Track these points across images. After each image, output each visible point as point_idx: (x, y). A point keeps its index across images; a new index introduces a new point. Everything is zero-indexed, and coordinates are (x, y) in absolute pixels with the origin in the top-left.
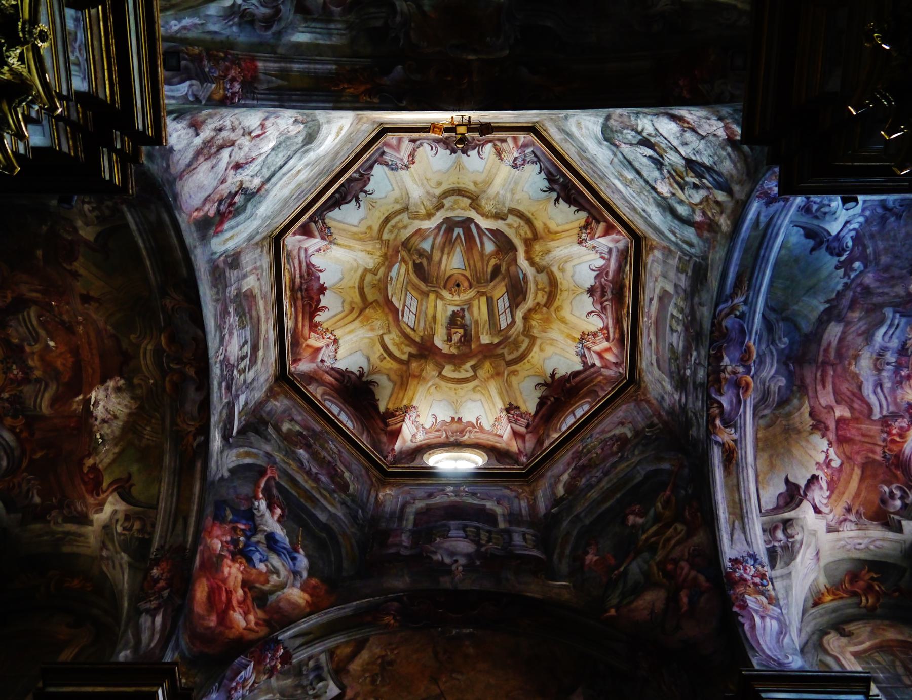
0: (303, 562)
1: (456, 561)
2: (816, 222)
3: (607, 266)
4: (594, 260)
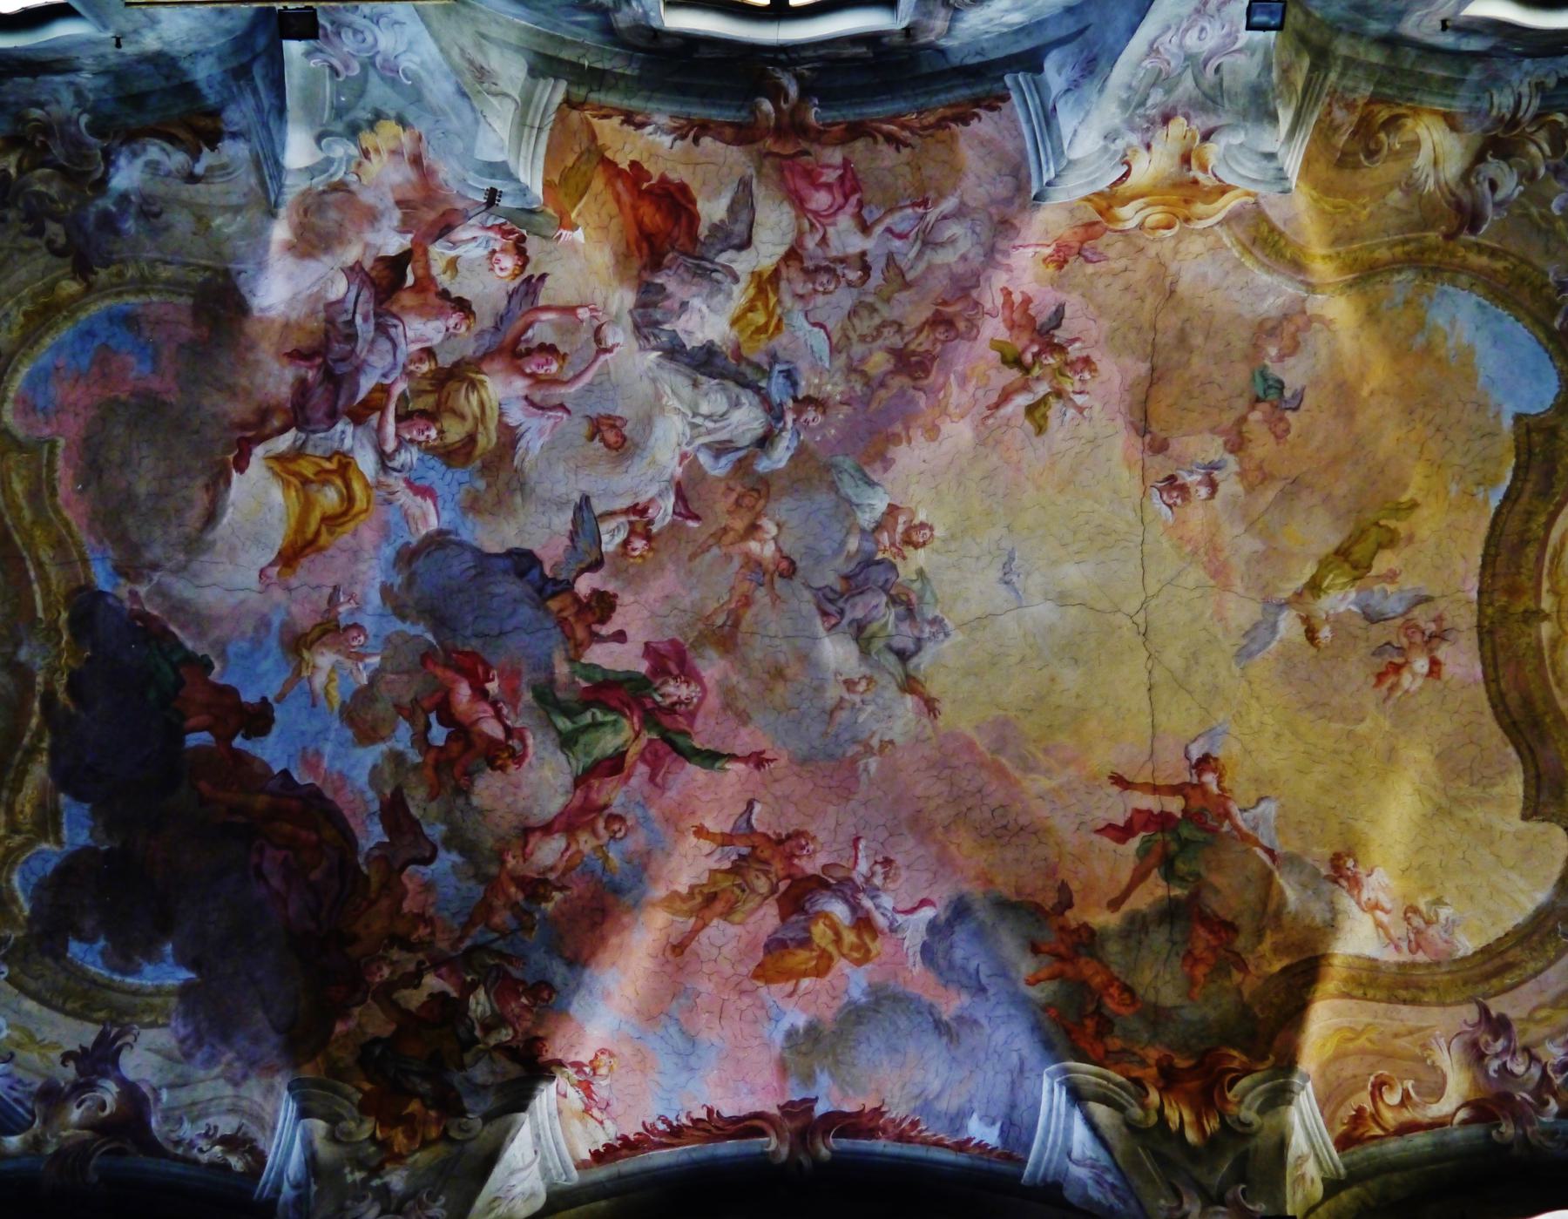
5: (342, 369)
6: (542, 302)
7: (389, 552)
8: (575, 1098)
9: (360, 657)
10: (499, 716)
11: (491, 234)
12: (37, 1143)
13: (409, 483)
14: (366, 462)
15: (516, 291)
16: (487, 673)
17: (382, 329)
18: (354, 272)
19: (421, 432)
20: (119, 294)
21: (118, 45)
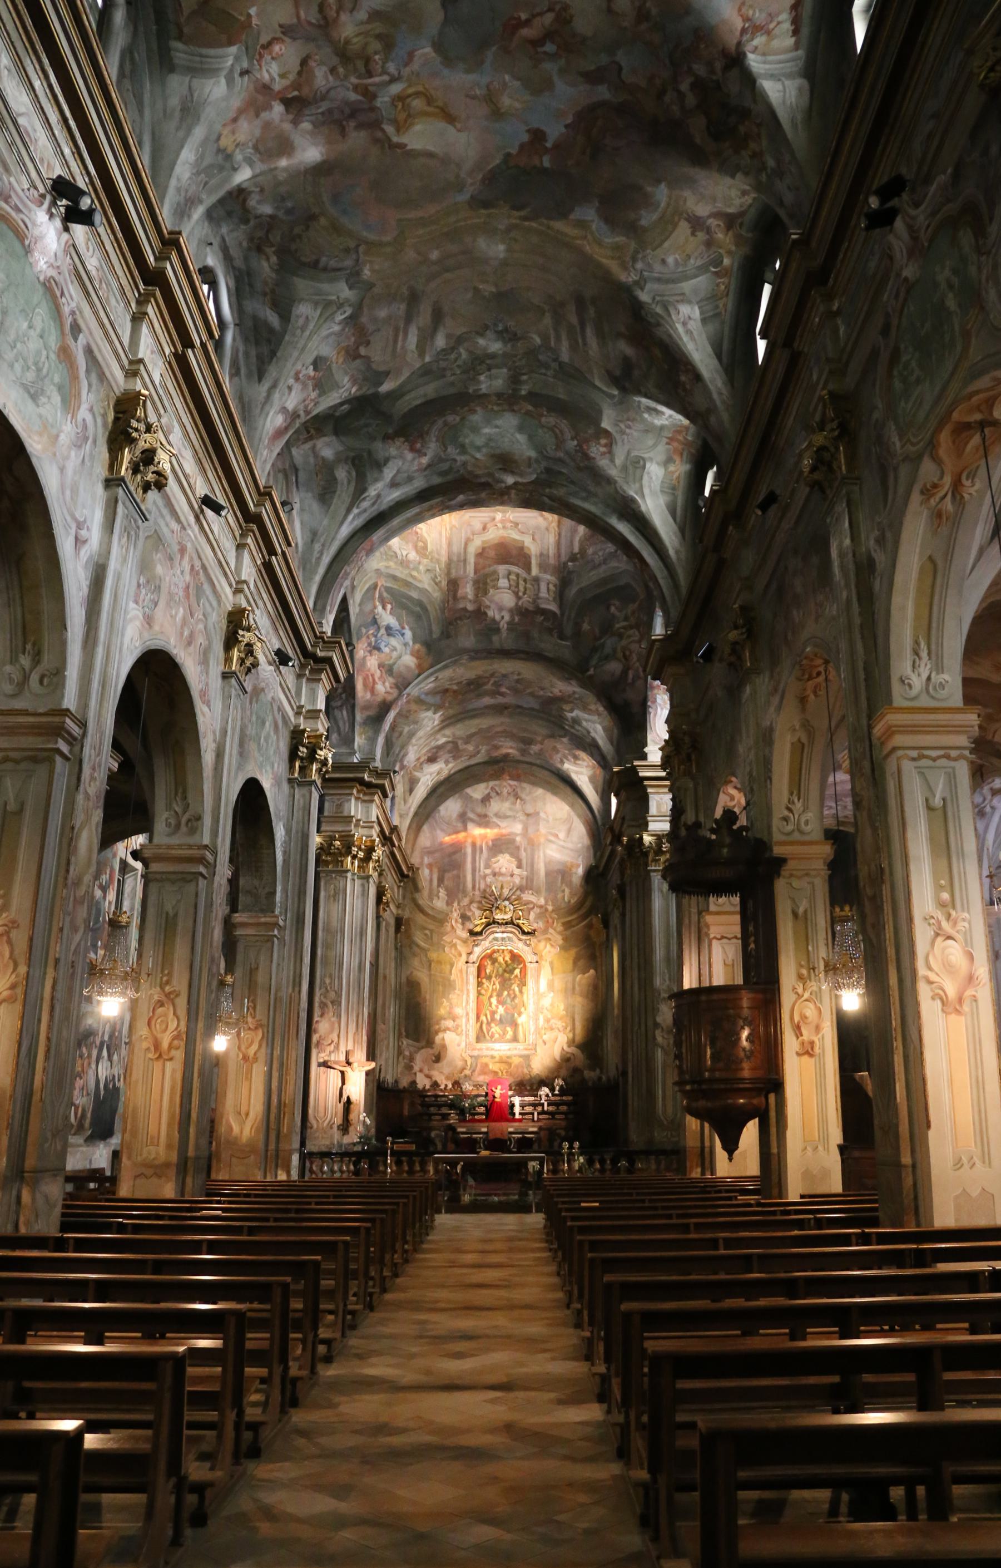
0: (408, 634)
1: (503, 617)
5: (347, 111)
6: (295, 20)
7: (446, 72)
8: (759, 40)
9: (505, 85)
10: (540, 14)
11: (263, 64)
12: (729, 253)
13: (406, 65)
14: (396, 89)
15: (291, 38)
16: (515, 19)
17: (323, 98)
18: (295, 123)
19: (377, 63)
20: (323, 202)
21: (211, 244)
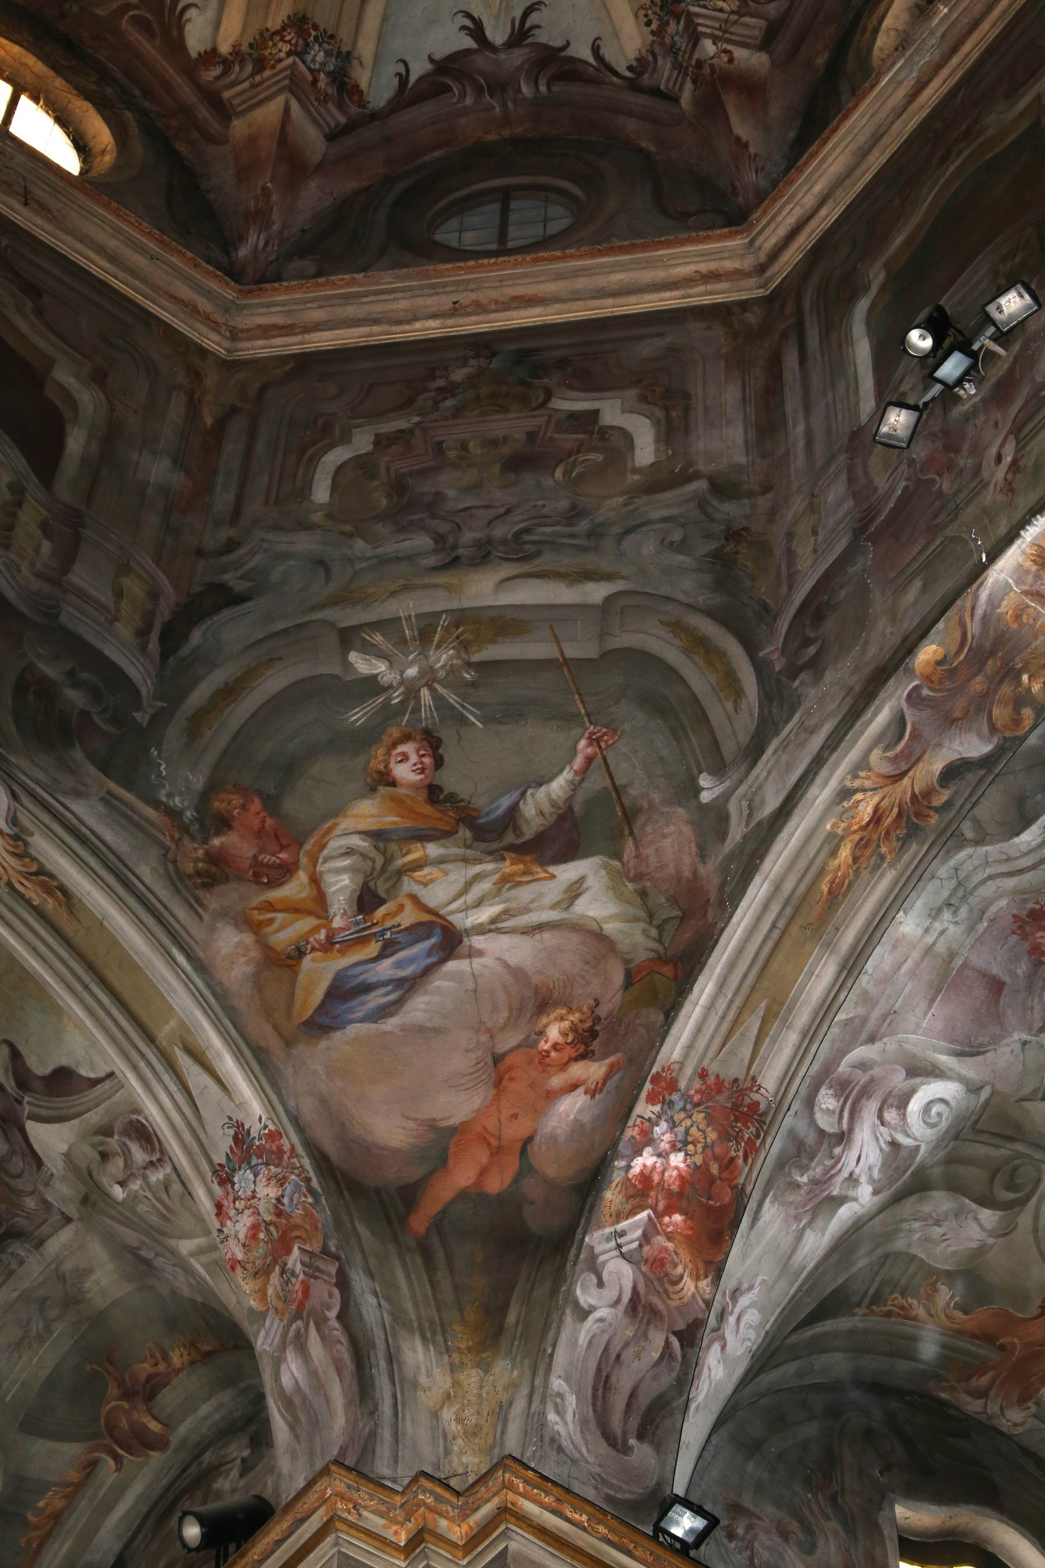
2: (94, 1117)
3: (176, 45)
4: (217, 24)
